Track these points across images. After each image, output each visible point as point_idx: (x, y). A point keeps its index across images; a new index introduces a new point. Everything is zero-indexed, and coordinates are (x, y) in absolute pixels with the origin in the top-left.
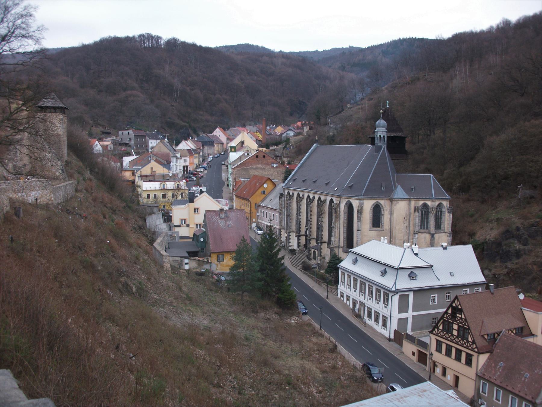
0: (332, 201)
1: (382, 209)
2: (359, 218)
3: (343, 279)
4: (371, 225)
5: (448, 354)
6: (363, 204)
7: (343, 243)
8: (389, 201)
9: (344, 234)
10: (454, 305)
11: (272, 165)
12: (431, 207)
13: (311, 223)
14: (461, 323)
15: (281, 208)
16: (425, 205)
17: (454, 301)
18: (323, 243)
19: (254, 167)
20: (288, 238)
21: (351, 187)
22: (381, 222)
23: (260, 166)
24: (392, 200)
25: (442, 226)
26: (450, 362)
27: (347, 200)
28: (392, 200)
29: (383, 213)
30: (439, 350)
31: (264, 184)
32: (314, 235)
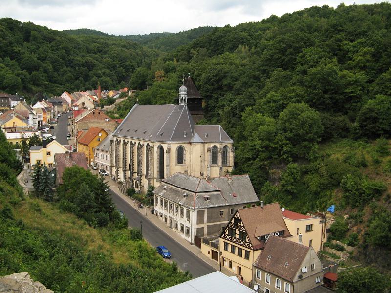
0: (148, 145)
2: (169, 158)
3: (157, 202)
5: (233, 252)
8: (189, 144)
10: (235, 217)
11: (105, 119)
14: (241, 229)
16: (215, 147)
17: (235, 214)
19: (92, 121)
20: (117, 173)
21: (162, 134)
23: (96, 120)
25: (228, 161)
26: (234, 258)
27: (159, 144)
30: (226, 249)
32: (136, 170)
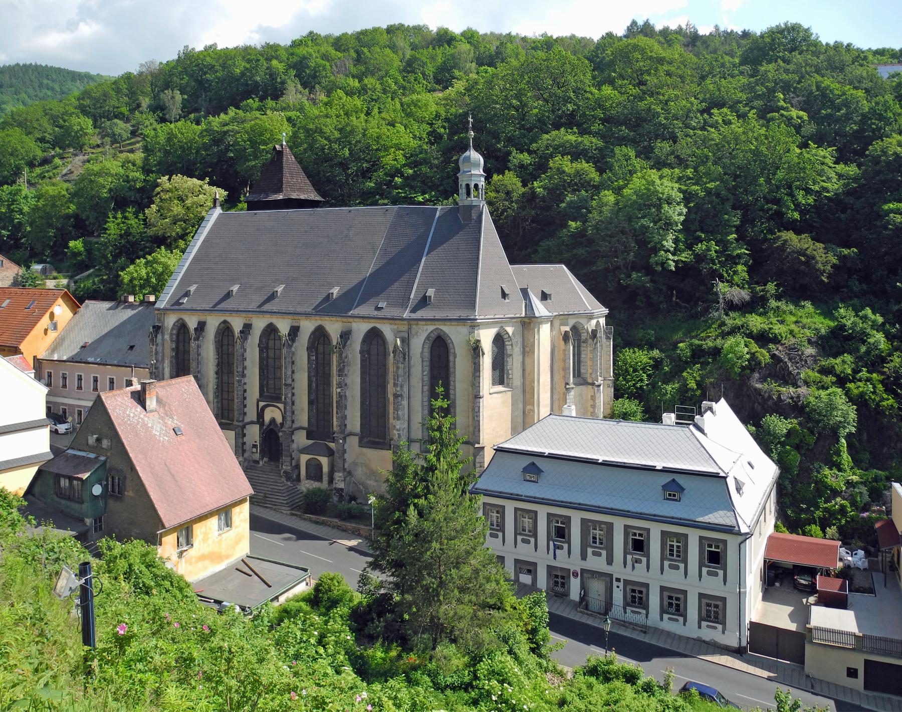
1: (506, 343)
4: (491, 382)
7: (423, 432)
9: (423, 409)
13: (293, 391)
18: (347, 438)
29: (509, 352)
32: (303, 419)
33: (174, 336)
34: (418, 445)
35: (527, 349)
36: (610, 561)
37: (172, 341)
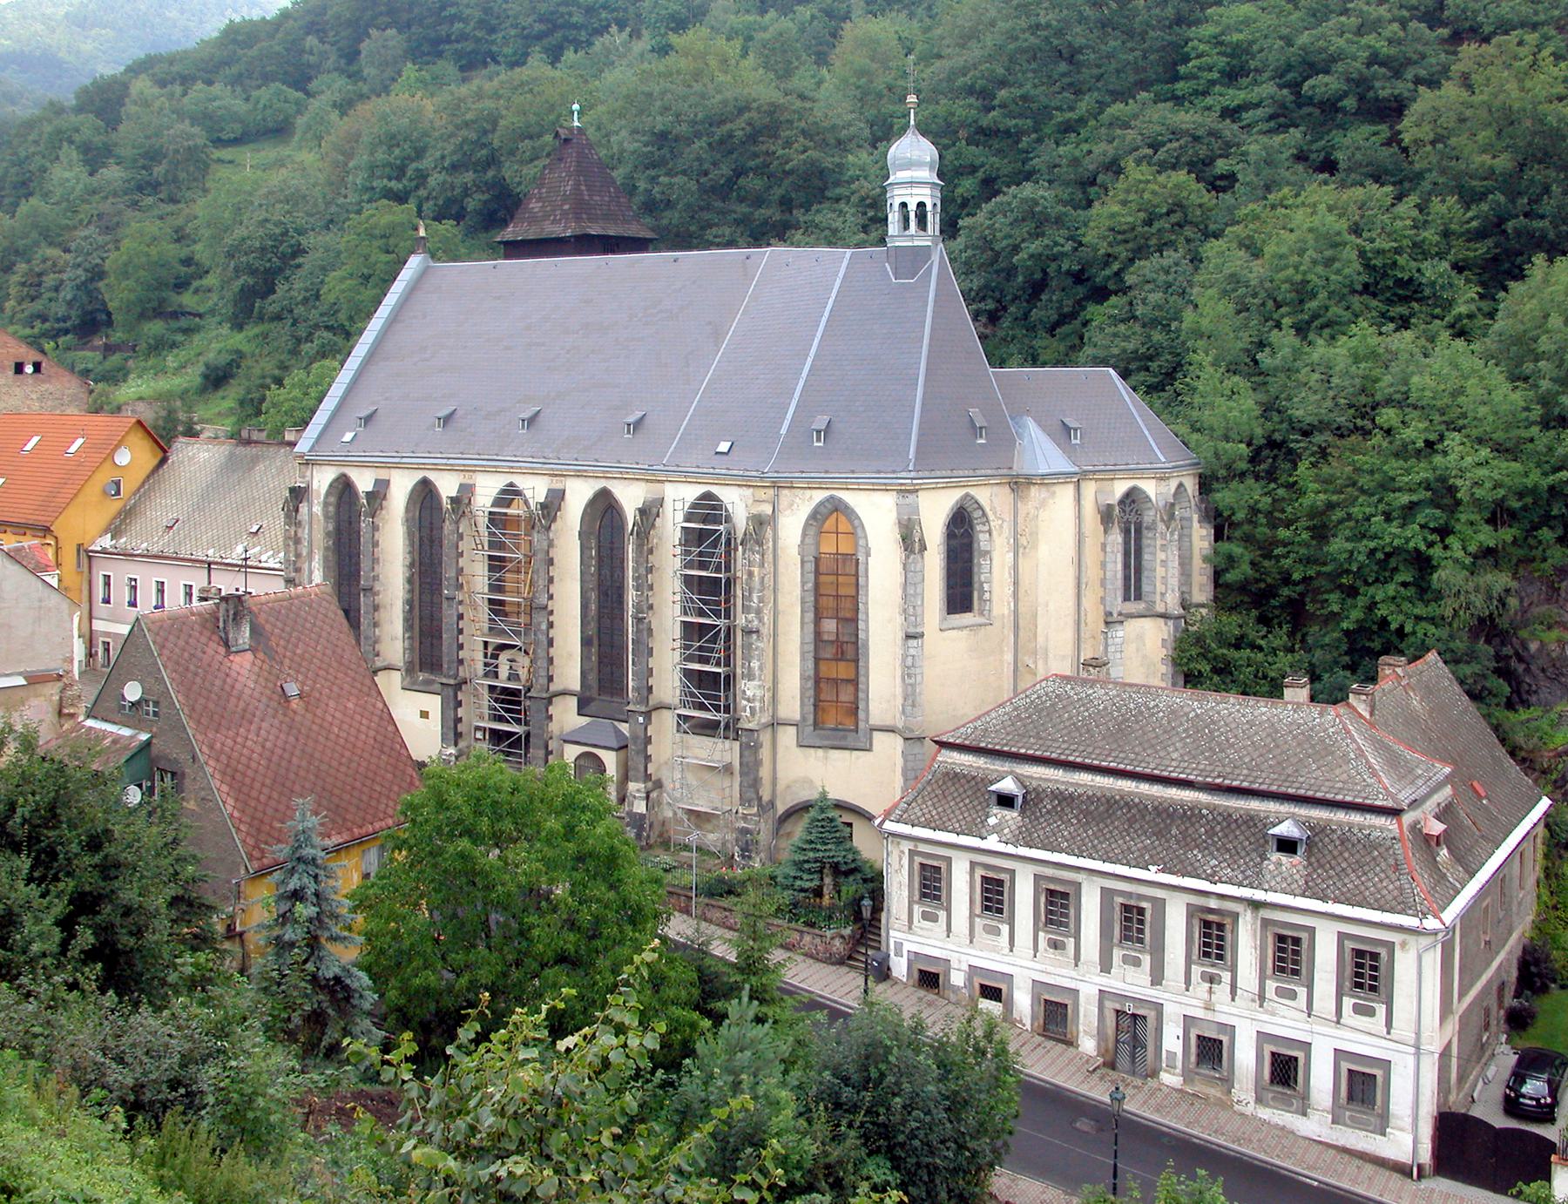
1: (979, 528)
6: (916, 510)
8: (1007, 489)
12: (1161, 504)
15: (298, 555)
18: (654, 714)
22: (976, 586)
24: (1019, 484)
27: (820, 496)
28: (1019, 484)
31: (117, 447)
32: (569, 669)
33: (331, 509)
34: (793, 730)
35: (1023, 541)
36: (1157, 978)
37: (326, 516)
